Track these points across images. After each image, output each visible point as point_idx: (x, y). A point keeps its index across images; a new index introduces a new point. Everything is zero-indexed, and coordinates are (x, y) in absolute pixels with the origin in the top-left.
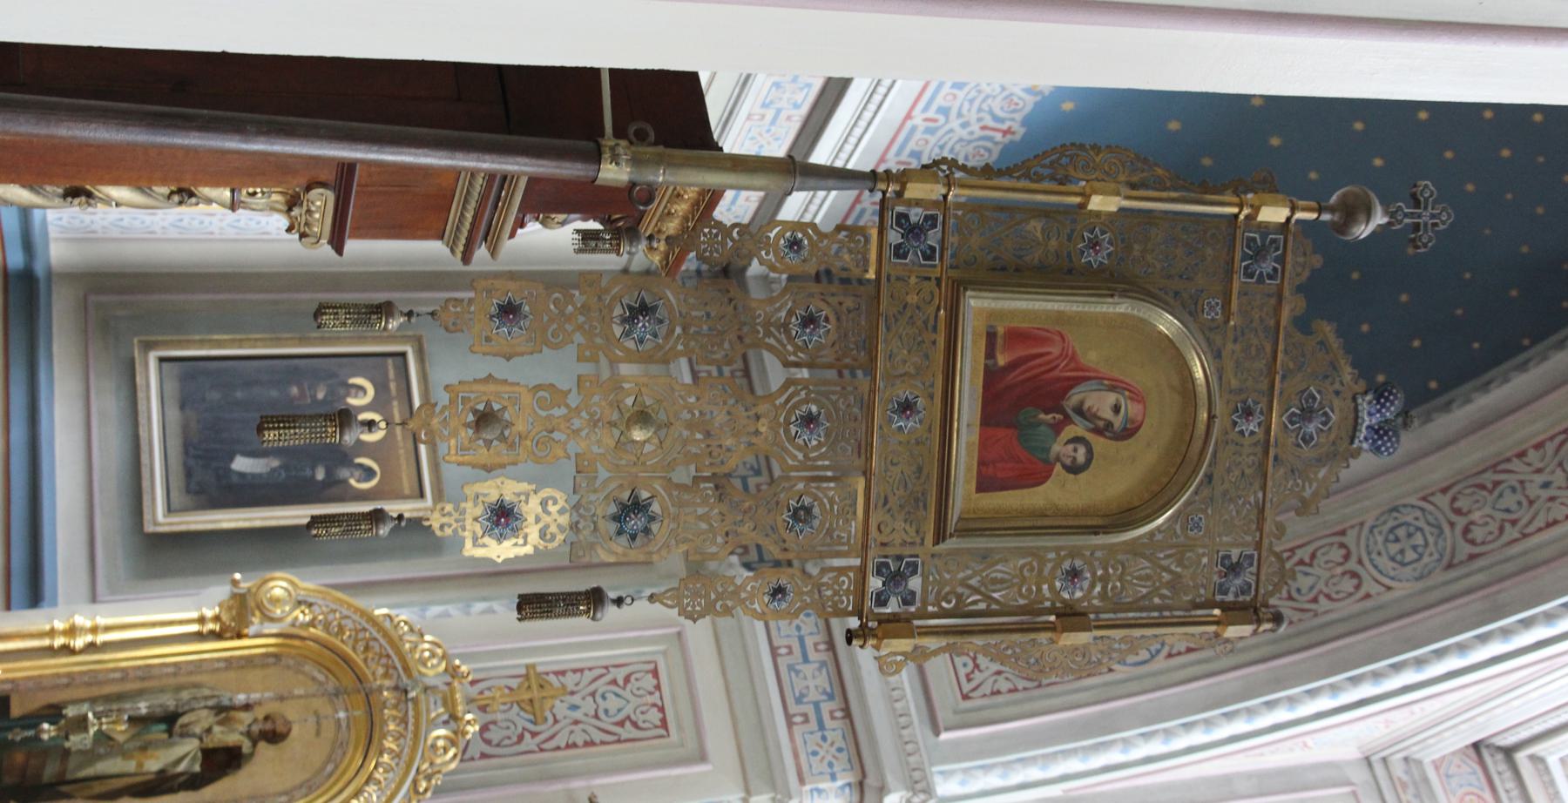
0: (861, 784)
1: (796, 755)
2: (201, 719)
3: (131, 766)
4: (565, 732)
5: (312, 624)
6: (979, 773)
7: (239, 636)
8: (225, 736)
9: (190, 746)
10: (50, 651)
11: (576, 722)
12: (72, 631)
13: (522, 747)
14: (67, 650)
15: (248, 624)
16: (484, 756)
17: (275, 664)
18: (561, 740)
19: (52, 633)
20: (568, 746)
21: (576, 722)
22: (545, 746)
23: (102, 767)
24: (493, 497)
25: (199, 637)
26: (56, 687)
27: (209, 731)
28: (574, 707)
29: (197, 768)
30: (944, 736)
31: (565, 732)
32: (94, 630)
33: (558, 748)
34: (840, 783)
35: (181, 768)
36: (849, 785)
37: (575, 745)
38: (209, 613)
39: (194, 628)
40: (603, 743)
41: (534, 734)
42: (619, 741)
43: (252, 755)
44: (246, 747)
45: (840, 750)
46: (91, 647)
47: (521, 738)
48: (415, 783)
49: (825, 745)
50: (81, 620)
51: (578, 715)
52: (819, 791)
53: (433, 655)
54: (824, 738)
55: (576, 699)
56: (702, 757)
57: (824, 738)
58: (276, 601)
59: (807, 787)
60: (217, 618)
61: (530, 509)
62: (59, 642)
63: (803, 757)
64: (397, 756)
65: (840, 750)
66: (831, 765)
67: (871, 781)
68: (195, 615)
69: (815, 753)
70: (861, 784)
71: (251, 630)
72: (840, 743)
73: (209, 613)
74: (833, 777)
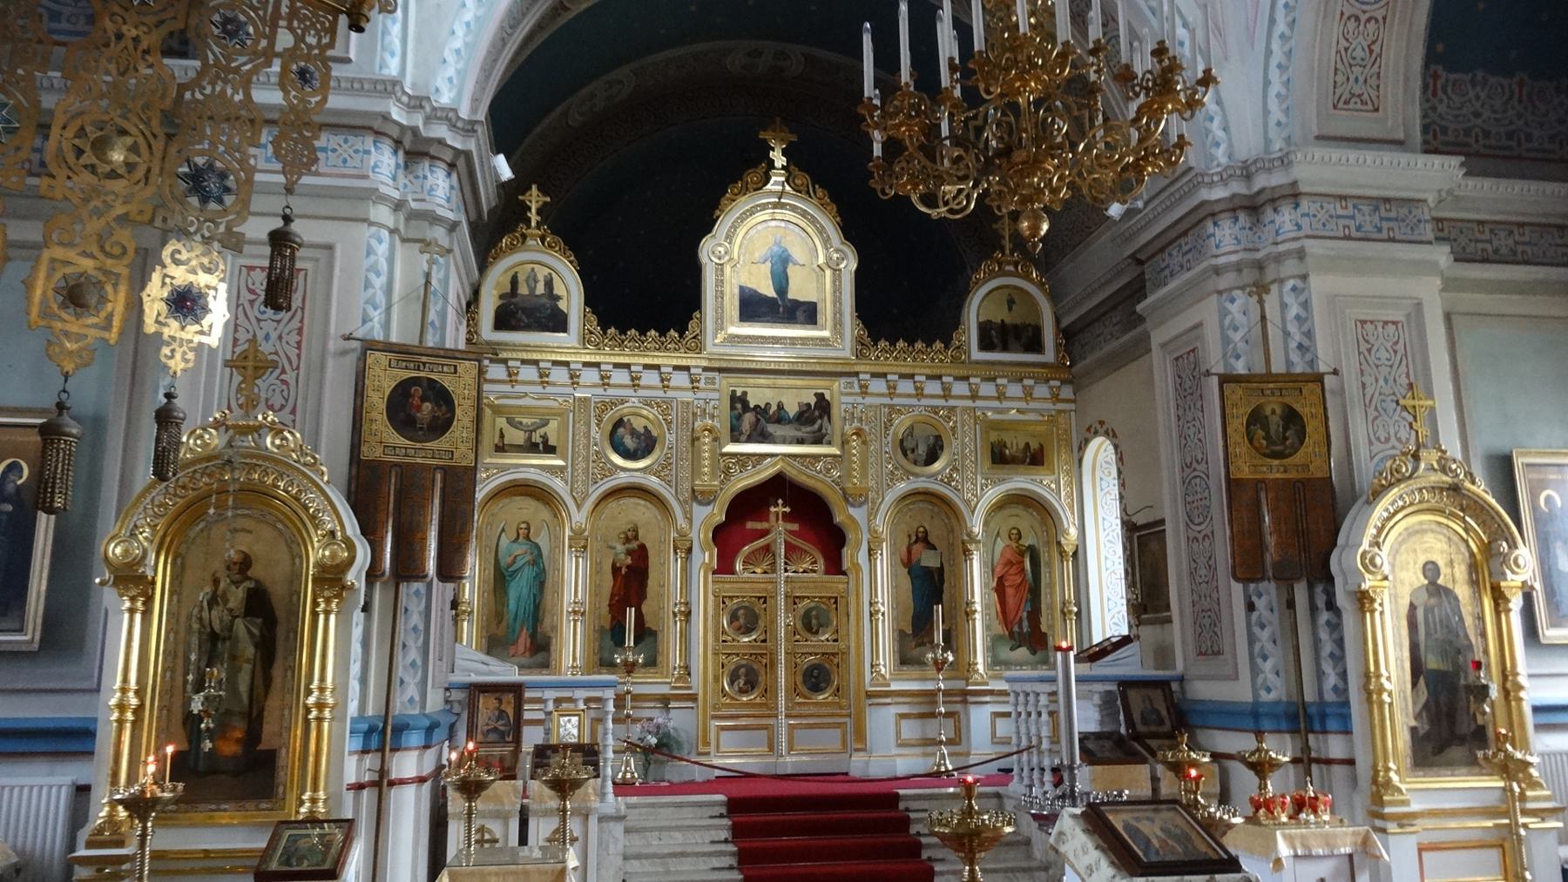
0: (377, 133)
1: (344, 176)
2: (217, 617)
3: (247, 667)
4: (286, 347)
5: (153, 527)
6: (387, 38)
7: (153, 583)
8: (237, 597)
9: (240, 626)
10: (137, 723)
11: (280, 338)
12: (122, 707)
13: (292, 382)
14: (138, 711)
15: (143, 577)
16: (293, 412)
17: (183, 558)
18: (293, 353)
19: (121, 722)
20: (299, 348)
21: (280, 338)
22: (295, 365)
23: (243, 688)
24: (163, 307)
25: (147, 614)
26: (169, 720)
27: (231, 610)
28: (267, 337)
29: (259, 621)
30: (352, 55)
31: (286, 347)
32: (124, 690)
33: (299, 356)
34: (373, 149)
35: (256, 631)
36: (375, 142)
37: (299, 343)
38: (127, 604)
39: (138, 617)
40: (302, 321)
41: (283, 371)
42: (303, 309)
43: (257, 581)
44: (247, 584)
45: (346, 141)
46: (140, 693)
47: (284, 382)
48: (305, 465)
49: (340, 151)
50: (113, 702)
51: (274, 335)
52: (376, 166)
53: (201, 437)
54: (334, 150)
55: (260, 335)
56: (329, 248)
57: (334, 150)
58: (126, 552)
59: (371, 174)
60: (133, 599)
61: (180, 276)
62: (129, 716)
63: (346, 171)
64: (281, 476)
65: (346, 141)
66: (356, 151)
67: (377, 125)
68: (126, 616)
69: (345, 161)
70: (377, 133)
71: (150, 574)
72: (340, 139)
73: (127, 604)
74: (367, 152)
